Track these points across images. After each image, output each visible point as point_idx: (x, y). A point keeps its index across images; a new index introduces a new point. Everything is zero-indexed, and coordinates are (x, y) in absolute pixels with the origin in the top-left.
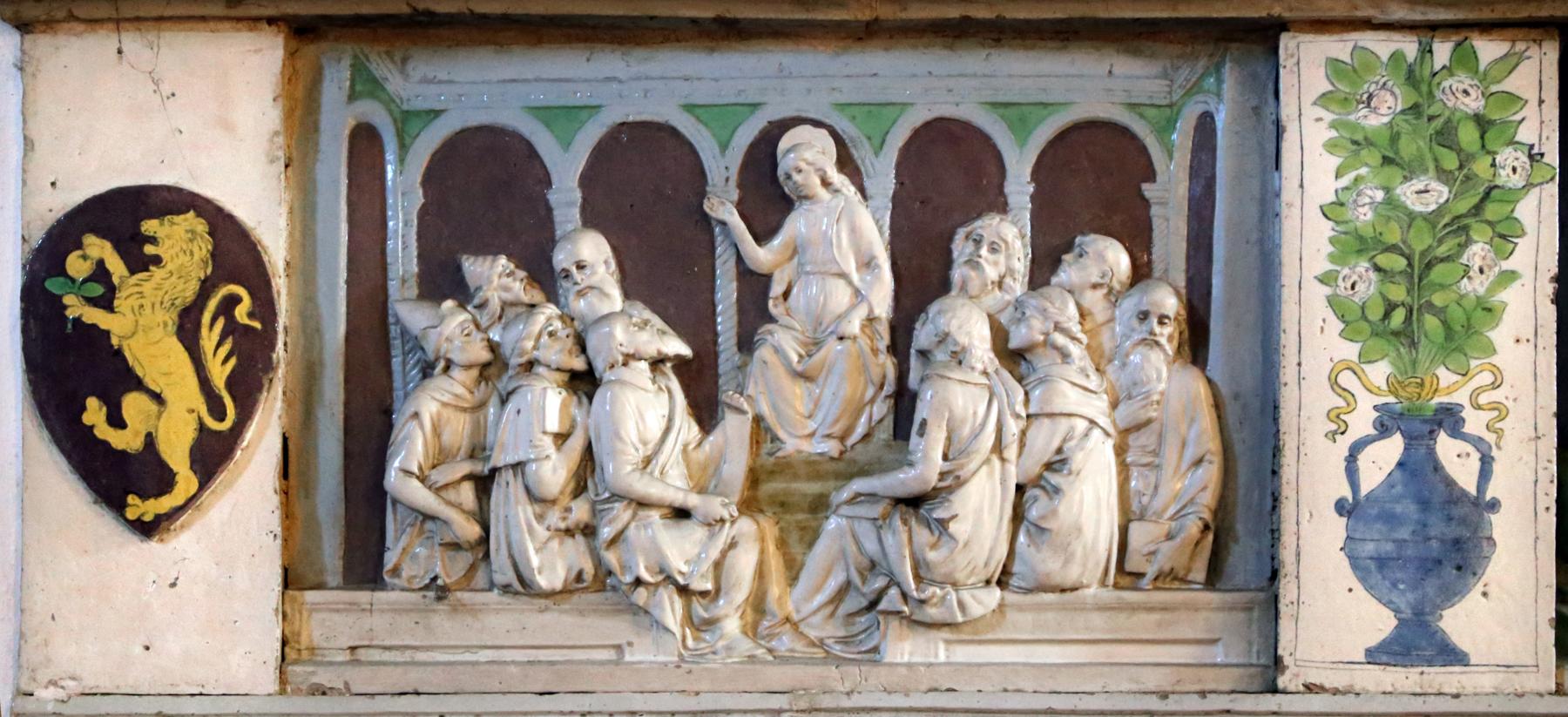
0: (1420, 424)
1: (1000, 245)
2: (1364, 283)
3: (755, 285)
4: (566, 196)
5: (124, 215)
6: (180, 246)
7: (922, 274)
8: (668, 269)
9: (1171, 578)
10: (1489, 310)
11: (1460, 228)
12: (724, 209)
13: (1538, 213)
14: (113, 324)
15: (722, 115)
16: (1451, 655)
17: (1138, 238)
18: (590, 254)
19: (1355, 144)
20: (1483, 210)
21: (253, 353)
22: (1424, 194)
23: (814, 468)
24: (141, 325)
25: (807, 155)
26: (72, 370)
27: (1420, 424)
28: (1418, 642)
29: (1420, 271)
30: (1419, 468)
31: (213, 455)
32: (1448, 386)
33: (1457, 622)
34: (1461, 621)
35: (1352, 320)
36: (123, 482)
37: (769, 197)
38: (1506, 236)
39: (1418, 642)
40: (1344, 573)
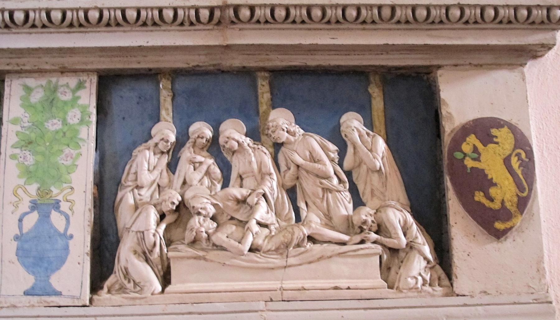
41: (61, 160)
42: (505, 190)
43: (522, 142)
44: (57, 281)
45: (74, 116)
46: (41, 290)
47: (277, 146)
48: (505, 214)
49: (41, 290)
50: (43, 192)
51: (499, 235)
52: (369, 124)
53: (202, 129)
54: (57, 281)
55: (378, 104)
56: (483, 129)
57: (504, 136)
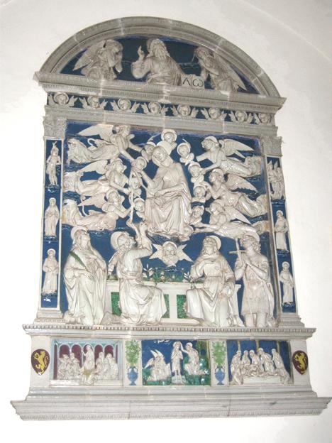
0: (133, 368)
1: (102, 355)
2: (128, 358)
3: (85, 357)
4: (70, 350)
5: (39, 351)
6: (43, 353)
7: (97, 356)
8: (78, 356)
9: (115, 379)
10: (137, 359)
11: (135, 353)
12: (82, 351)
13: (140, 352)
14: (38, 359)
15: (82, 345)
16: (135, 385)
17: (112, 354)
18: (72, 355)
19: (128, 347)
20: (136, 352)
21: (48, 362)
22: (133, 351)
23: (89, 370)
24: (40, 359)
25: (88, 348)
26: (34, 363)
27: (133, 368)
28: (133, 384)
29: (133, 356)
30: (133, 370)
31: (45, 369)
32: (134, 365)
33: (136, 382)
34: (136, 382)
35: (128, 360)
36: (37, 371)
37: (85, 351)
38: (138, 354)
39: (133, 384)
40: (127, 379)
41: (222, 358)
42: (303, 365)
43: (306, 356)
44: (223, 382)
45: (223, 349)
46: (220, 384)
47: (260, 356)
48: (303, 370)
49: (220, 384)
50: (219, 364)
51: (302, 374)
52: (277, 351)
53: (246, 352)
54: (223, 382)
55: (278, 347)
56: (299, 353)
57: (302, 354)
